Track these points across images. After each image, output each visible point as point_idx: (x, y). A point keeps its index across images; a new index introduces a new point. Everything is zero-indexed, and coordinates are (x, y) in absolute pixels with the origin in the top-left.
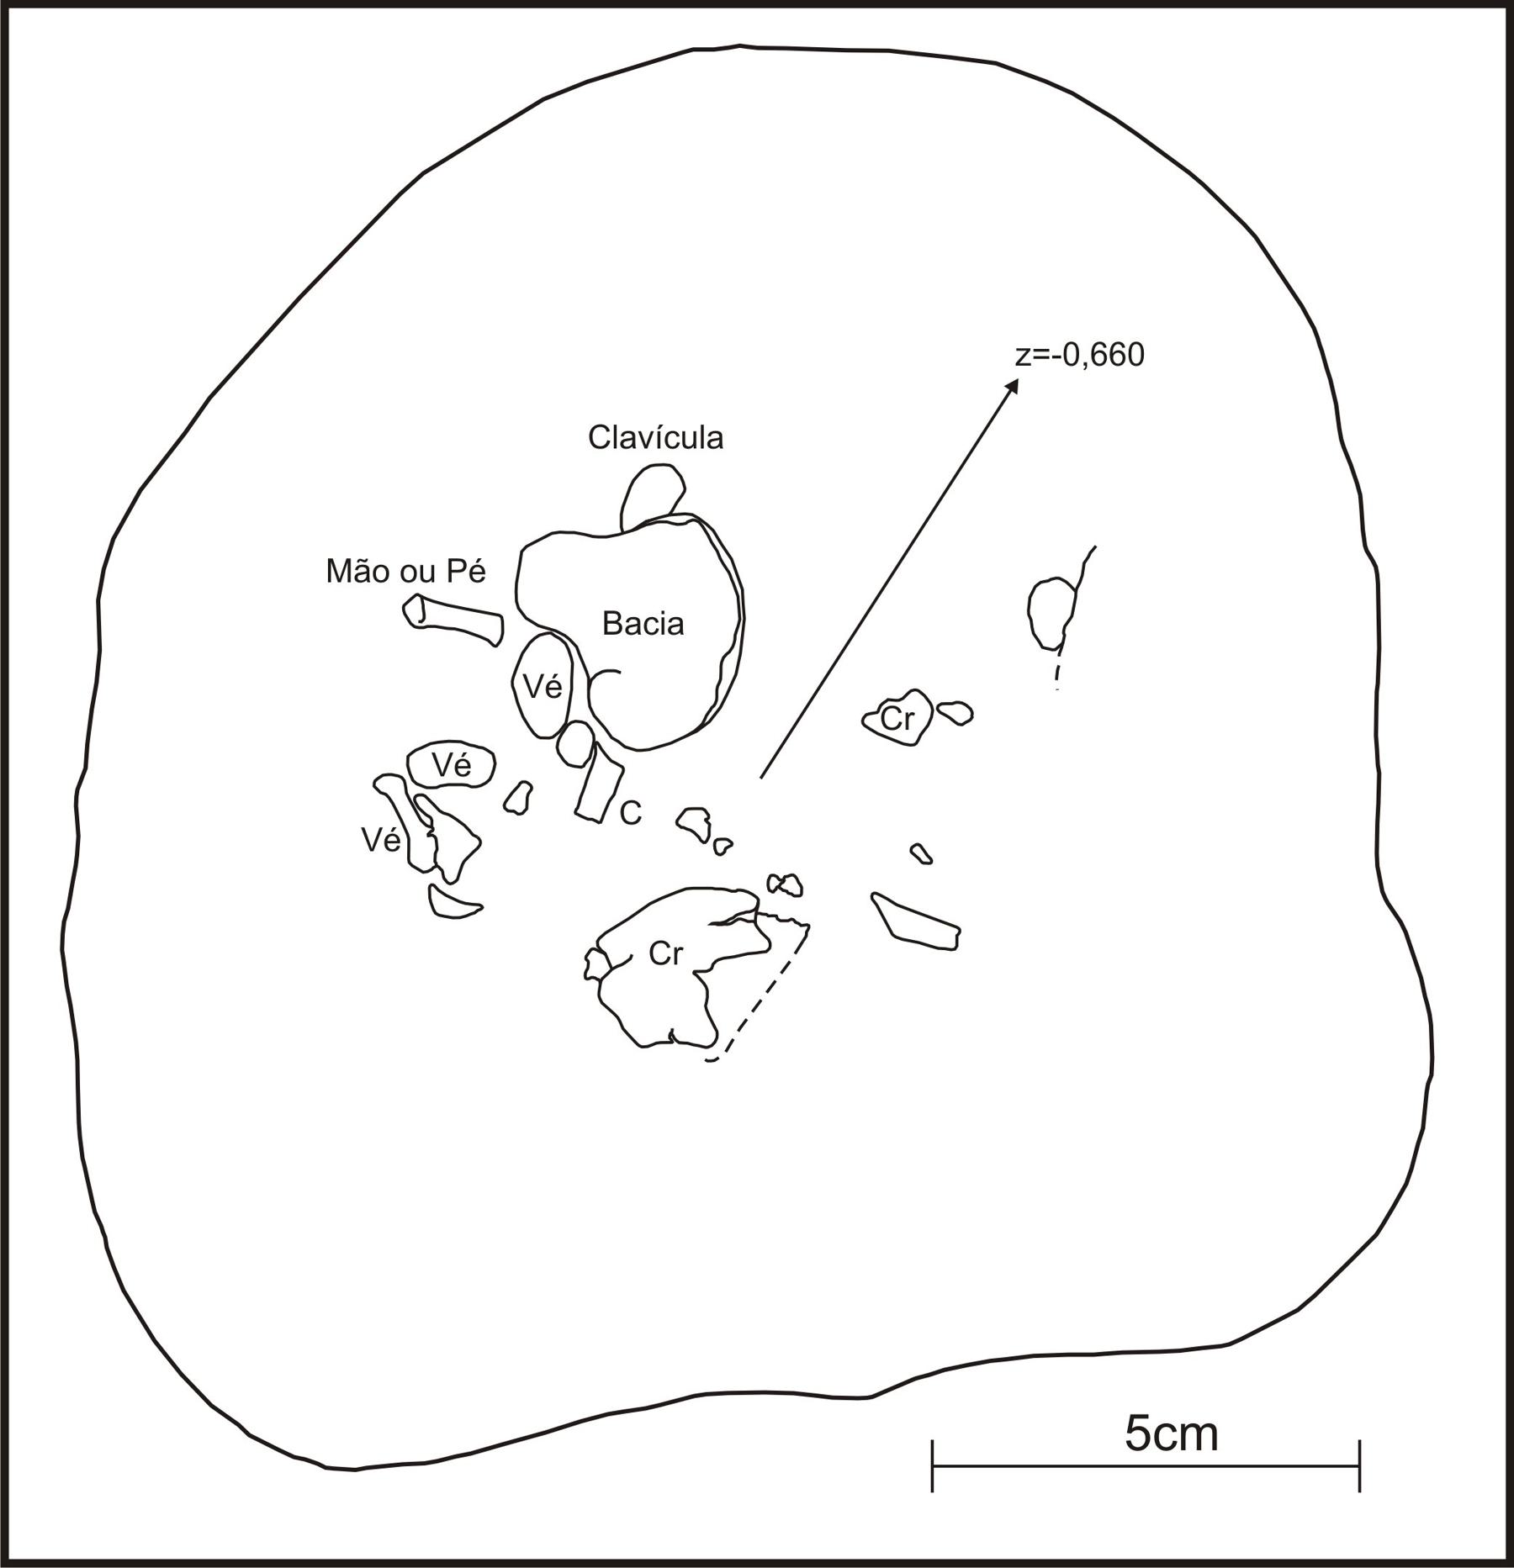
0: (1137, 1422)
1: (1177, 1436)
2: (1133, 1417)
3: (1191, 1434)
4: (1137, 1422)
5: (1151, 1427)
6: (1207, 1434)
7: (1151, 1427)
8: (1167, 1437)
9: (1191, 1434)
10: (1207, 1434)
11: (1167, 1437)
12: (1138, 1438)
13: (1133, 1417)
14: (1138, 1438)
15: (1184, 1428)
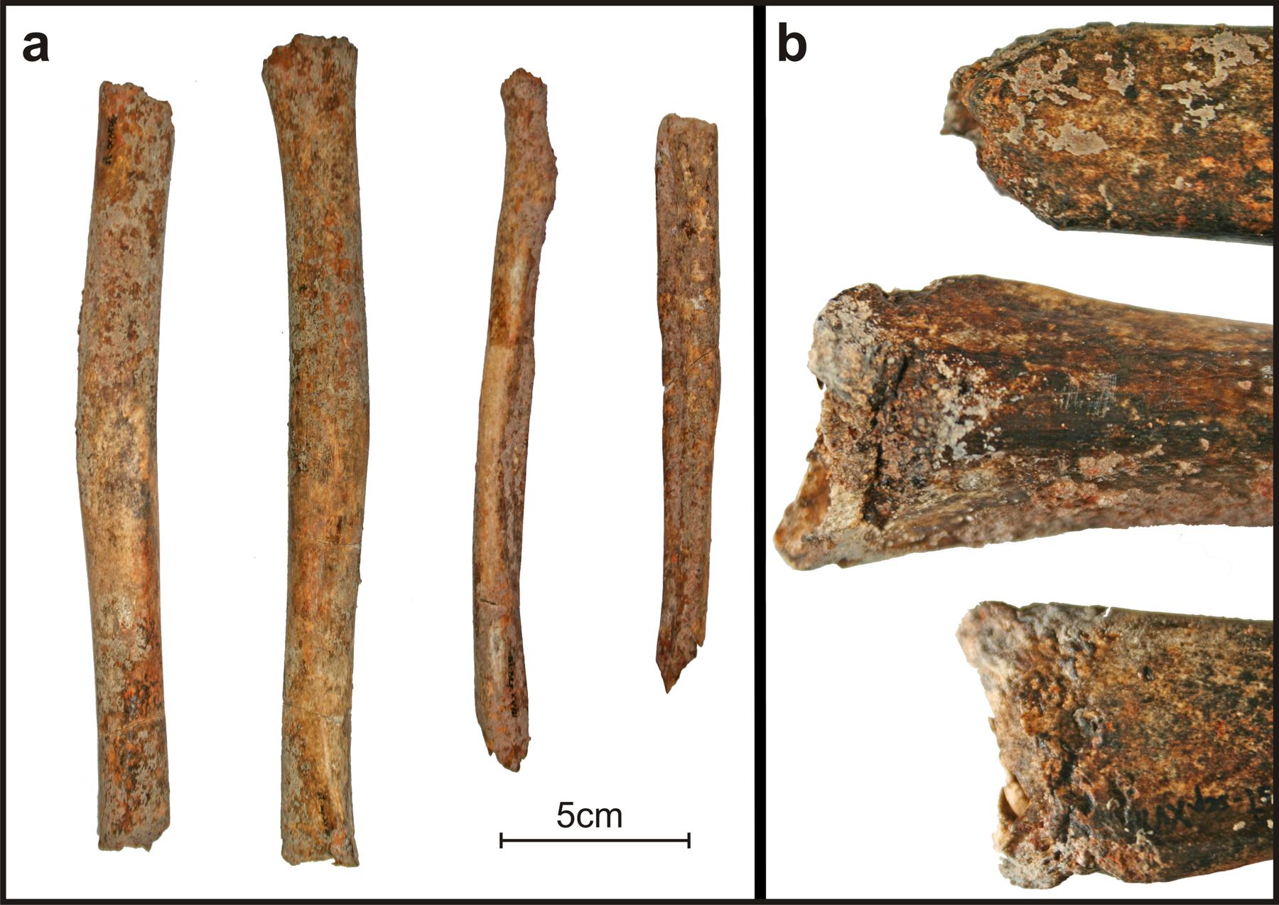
0: (565, 808)
1: (593, 818)
2: (562, 804)
3: (603, 815)
4: (565, 808)
5: (575, 810)
6: (614, 815)
7: (575, 810)
8: (586, 818)
9: (603, 815)
10: (614, 815)
11: (586, 818)
12: (566, 819)
13: (562, 804)
14: (566, 819)
15: (598, 812)
